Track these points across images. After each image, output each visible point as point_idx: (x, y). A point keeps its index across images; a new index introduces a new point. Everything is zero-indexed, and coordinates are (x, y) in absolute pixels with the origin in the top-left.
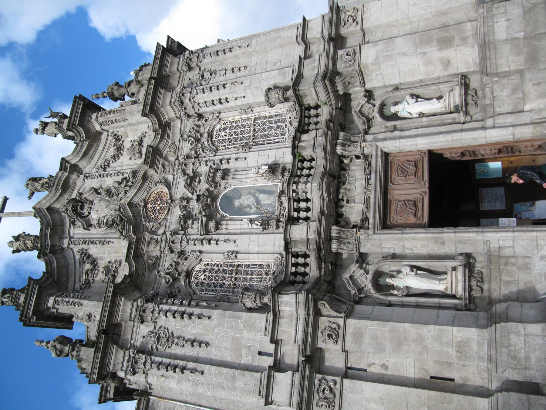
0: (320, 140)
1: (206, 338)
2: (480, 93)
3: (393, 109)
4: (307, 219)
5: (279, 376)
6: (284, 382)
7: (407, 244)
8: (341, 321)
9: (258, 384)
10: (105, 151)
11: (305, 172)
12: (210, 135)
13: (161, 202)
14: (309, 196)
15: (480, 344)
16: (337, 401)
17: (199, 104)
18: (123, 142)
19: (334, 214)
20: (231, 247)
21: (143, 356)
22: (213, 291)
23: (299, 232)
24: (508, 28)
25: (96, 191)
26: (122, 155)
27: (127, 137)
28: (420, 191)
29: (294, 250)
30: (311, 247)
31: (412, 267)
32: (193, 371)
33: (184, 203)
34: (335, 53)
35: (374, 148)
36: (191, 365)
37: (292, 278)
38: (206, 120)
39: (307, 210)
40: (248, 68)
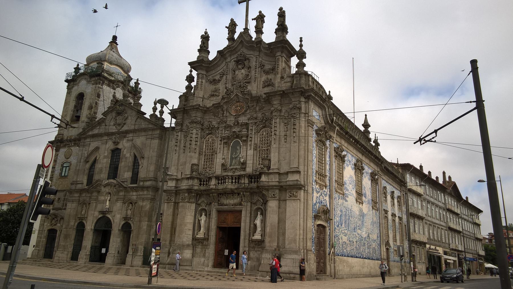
2: (260, 246)
3: (259, 213)
4: (219, 183)
5: (174, 182)
10: (269, 63)
20: (218, 152)
24: (267, 258)
25: (249, 67)
34: (277, 189)
40: (285, 144)
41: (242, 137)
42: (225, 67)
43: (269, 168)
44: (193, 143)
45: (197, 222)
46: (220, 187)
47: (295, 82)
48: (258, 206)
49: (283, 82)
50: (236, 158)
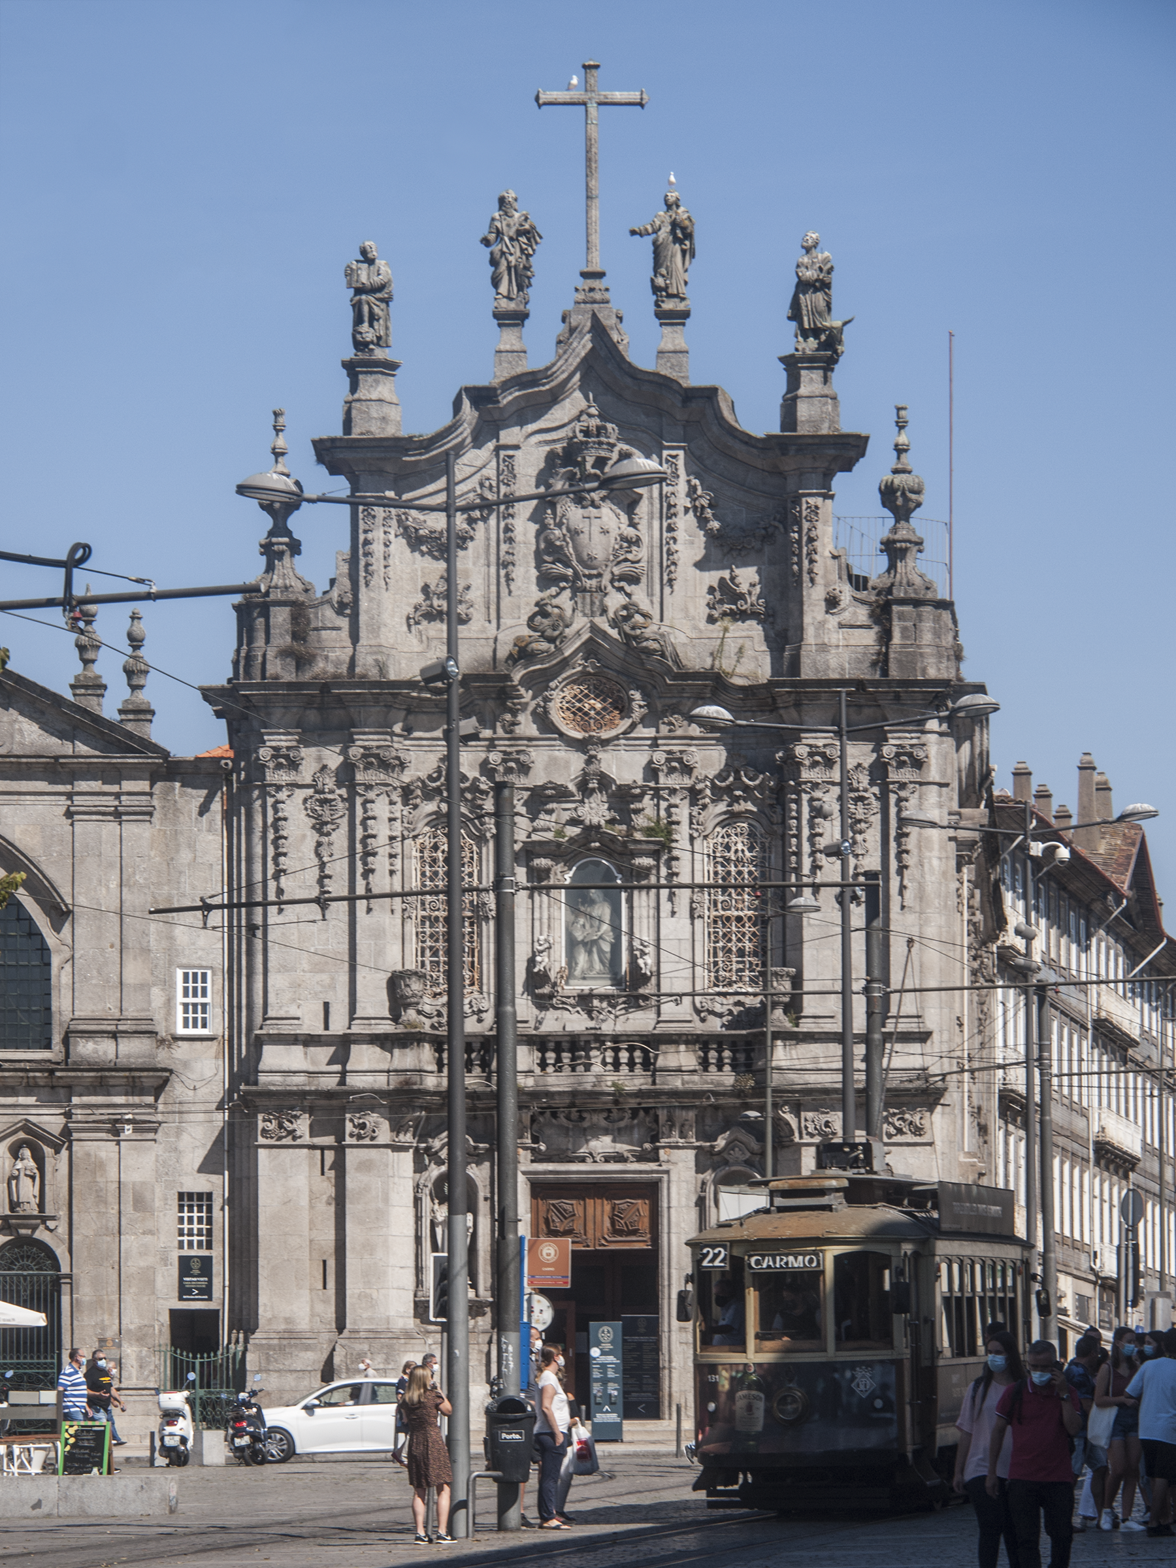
0: (677, 1083)
4: (543, 1065)
9: (282, 1014)
11: (624, 1056)
13: (598, 713)
15: (371, 1319)
22: (423, 874)
35: (664, 1168)
41: (633, 855)
42: (491, 471)
43: (794, 1007)
44: (380, 863)
46: (558, 1082)
47: (897, 639)
49: (833, 621)
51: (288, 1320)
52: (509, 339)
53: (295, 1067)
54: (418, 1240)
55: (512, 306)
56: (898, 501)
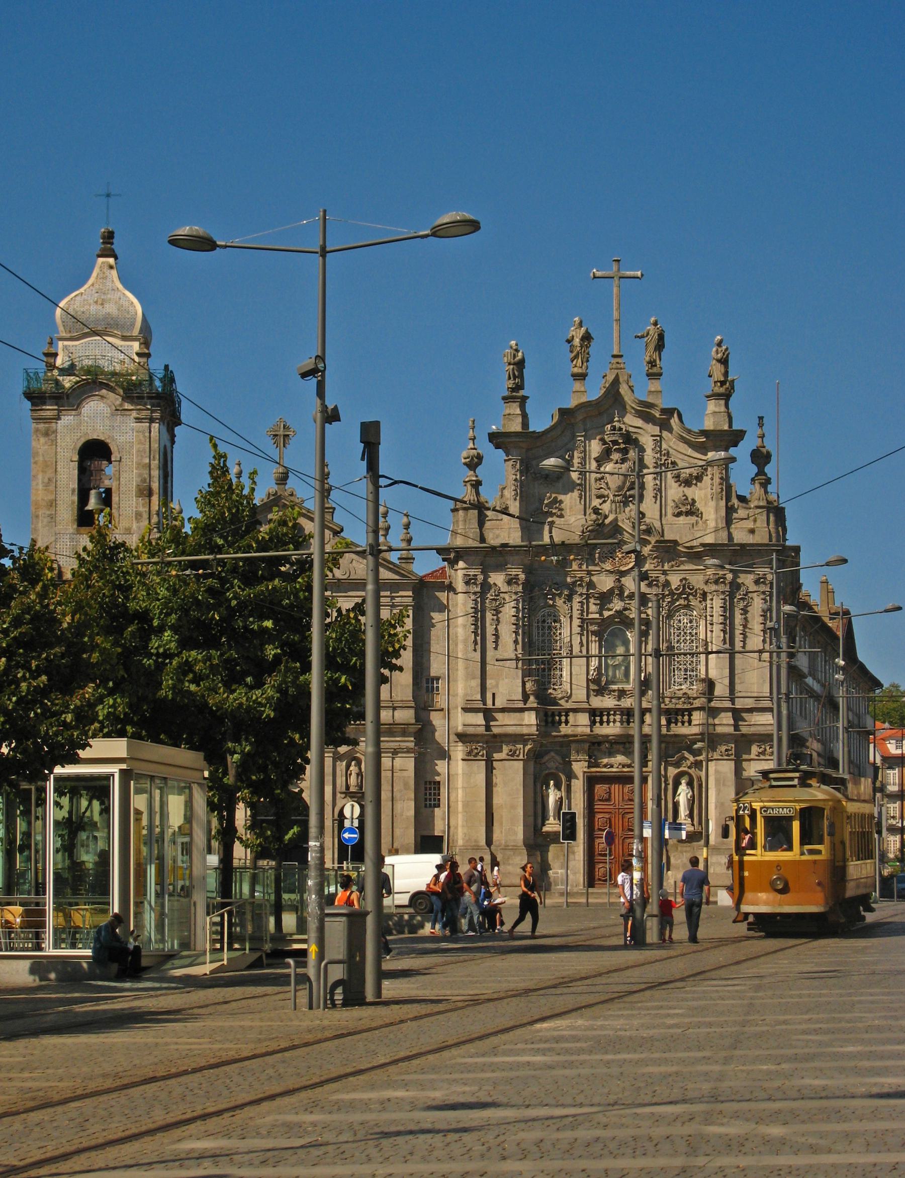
1: (499, 647)
6: (479, 719)
7: (578, 795)
8: (521, 757)
12: (688, 606)
14: (611, 724)
16: (472, 758)
17: (712, 600)
18: (696, 485)
19: (595, 747)
21: (478, 589)
23: (583, 719)
26: (680, 485)
27: (701, 489)
28: (617, 802)
29: (571, 714)
30: (573, 728)
31: (561, 798)
32: (475, 642)
33: (617, 592)
36: (479, 638)
37: (550, 713)
38: (700, 602)
39: (601, 723)
45: (539, 800)
48: (681, 769)
50: (615, 667)
51: (476, 841)
52: (577, 386)
53: (479, 723)
54: (535, 802)
55: (580, 371)
56: (760, 458)
